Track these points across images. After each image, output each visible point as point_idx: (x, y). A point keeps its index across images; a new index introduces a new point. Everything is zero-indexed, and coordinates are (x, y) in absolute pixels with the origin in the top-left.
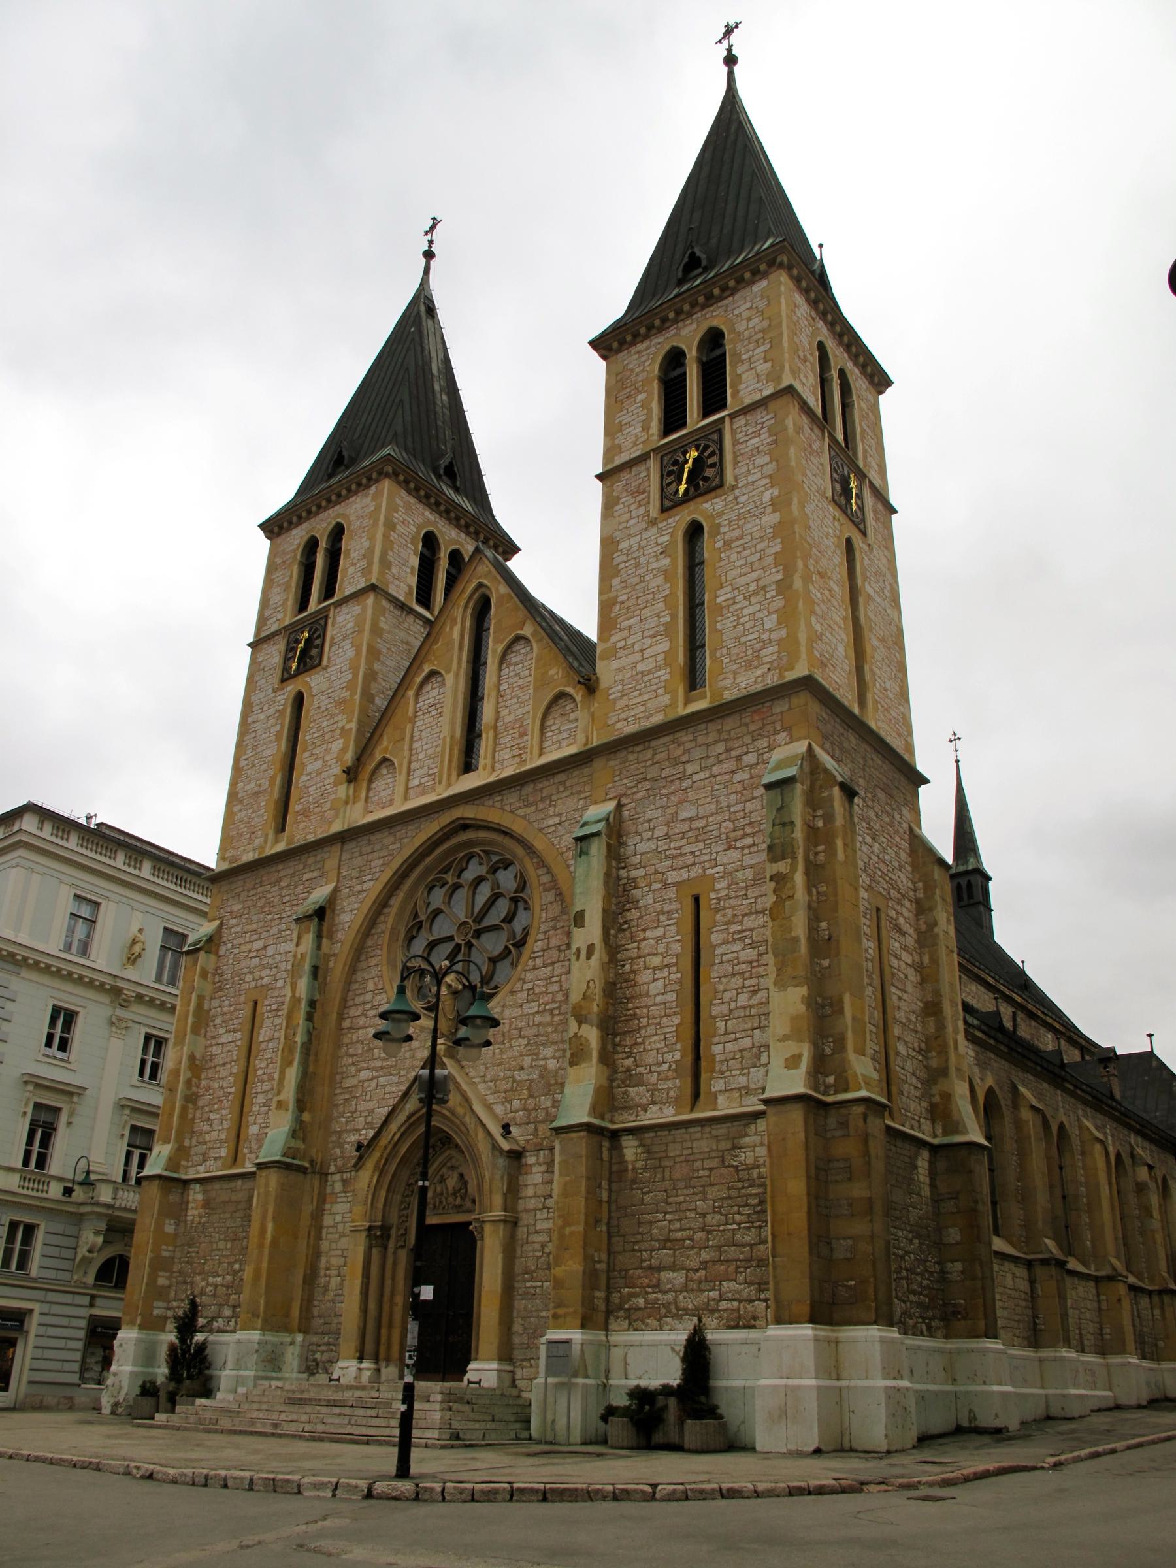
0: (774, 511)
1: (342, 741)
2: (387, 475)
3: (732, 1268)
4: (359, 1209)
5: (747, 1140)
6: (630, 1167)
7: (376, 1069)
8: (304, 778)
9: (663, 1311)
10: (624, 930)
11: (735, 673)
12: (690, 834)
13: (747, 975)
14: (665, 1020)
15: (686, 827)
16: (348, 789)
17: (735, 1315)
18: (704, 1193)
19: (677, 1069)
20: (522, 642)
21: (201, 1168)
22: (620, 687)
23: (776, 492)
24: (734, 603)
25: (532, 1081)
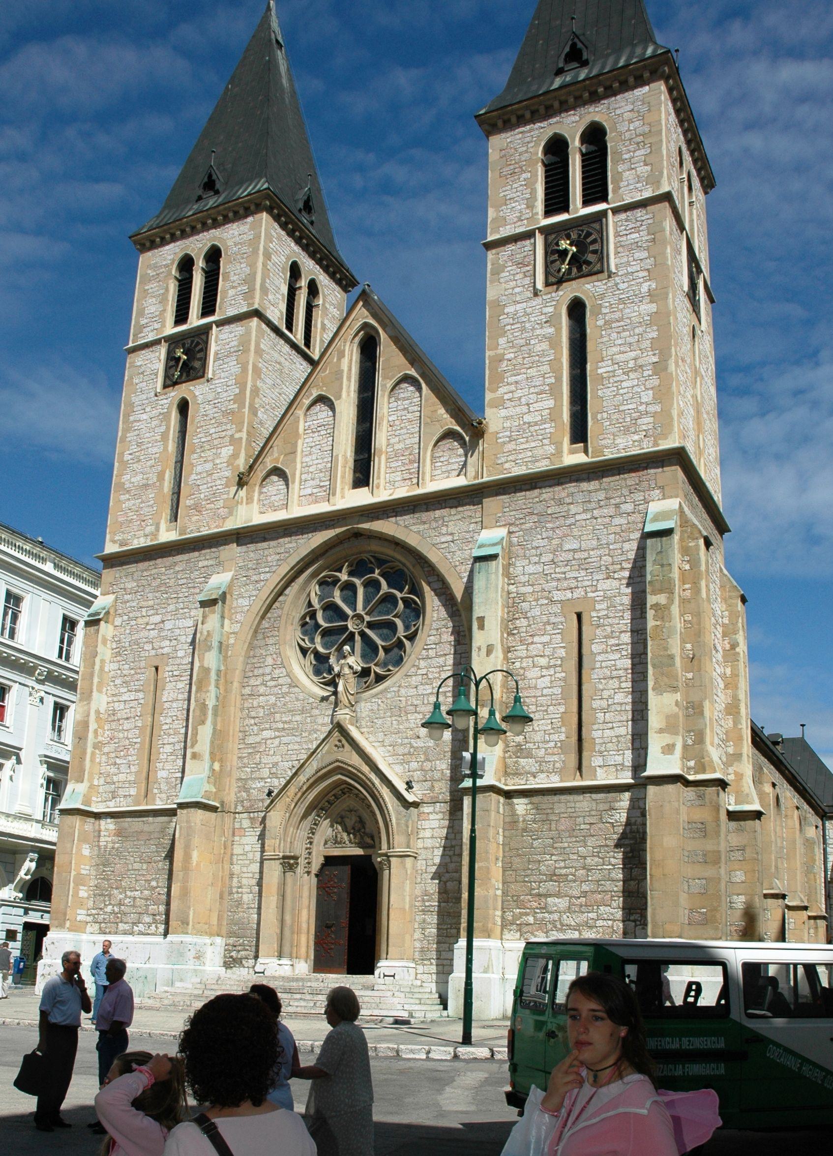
1: (232, 448)
6: (521, 819)
7: (278, 730)
8: (193, 477)
9: (550, 926)
12: (573, 562)
13: (623, 679)
14: (551, 708)
15: (570, 556)
19: (563, 747)
21: (112, 804)
22: (508, 433)
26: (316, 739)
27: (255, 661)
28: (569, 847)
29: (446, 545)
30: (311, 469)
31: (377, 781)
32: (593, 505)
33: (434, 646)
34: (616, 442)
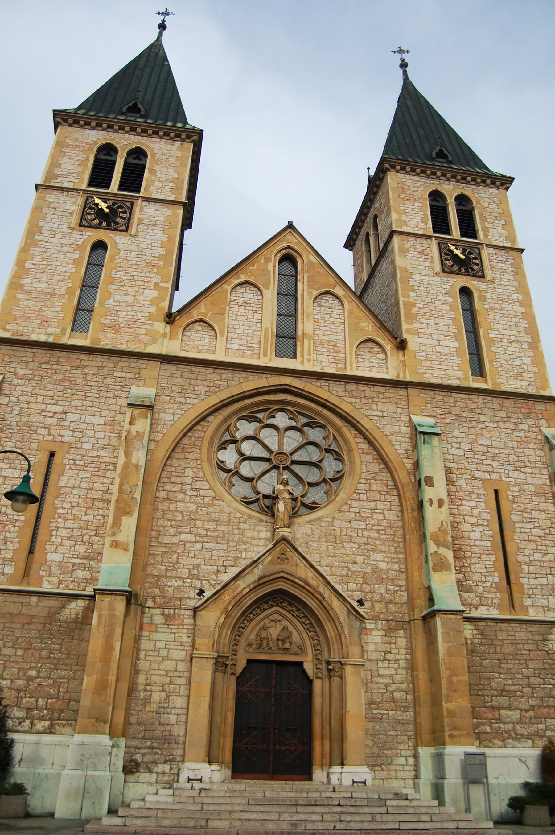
14: (484, 557)
26: (245, 550)
30: (237, 331)
31: (327, 593)
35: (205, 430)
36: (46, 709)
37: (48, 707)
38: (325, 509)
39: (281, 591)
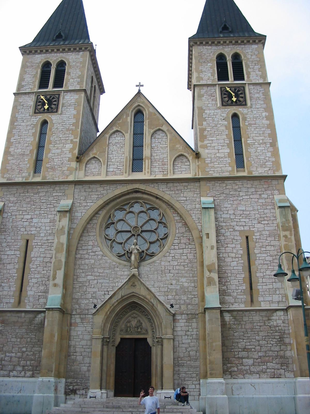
0: (267, 120)
2: (89, 50)
3: (271, 358)
4: (97, 330)
5: (273, 318)
6: (228, 323)
8: (50, 154)
9: (245, 372)
10: (219, 242)
11: (257, 167)
12: (243, 215)
13: (269, 265)
14: (238, 275)
16: (77, 164)
17: (273, 374)
18: (258, 333)
19: (244, 292)
20: (161, 131)
22: (210, 159)
23: (267, 114)
24: (254, 144)
25: (177, 289)
26: (117, 282)
27: (83, 242)
28: (251, 336)
29: (183, 201)
30: (112, 161)
32: (249, 193)
33: (178, 244)
34: (257, 170)
35: (98, 219)
36: (31, 366)
37: (31, 365)
38: (157, 256)
39: (134, 302)
